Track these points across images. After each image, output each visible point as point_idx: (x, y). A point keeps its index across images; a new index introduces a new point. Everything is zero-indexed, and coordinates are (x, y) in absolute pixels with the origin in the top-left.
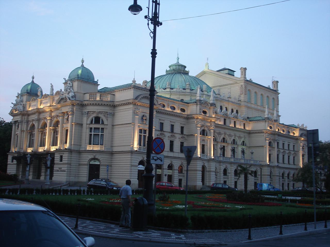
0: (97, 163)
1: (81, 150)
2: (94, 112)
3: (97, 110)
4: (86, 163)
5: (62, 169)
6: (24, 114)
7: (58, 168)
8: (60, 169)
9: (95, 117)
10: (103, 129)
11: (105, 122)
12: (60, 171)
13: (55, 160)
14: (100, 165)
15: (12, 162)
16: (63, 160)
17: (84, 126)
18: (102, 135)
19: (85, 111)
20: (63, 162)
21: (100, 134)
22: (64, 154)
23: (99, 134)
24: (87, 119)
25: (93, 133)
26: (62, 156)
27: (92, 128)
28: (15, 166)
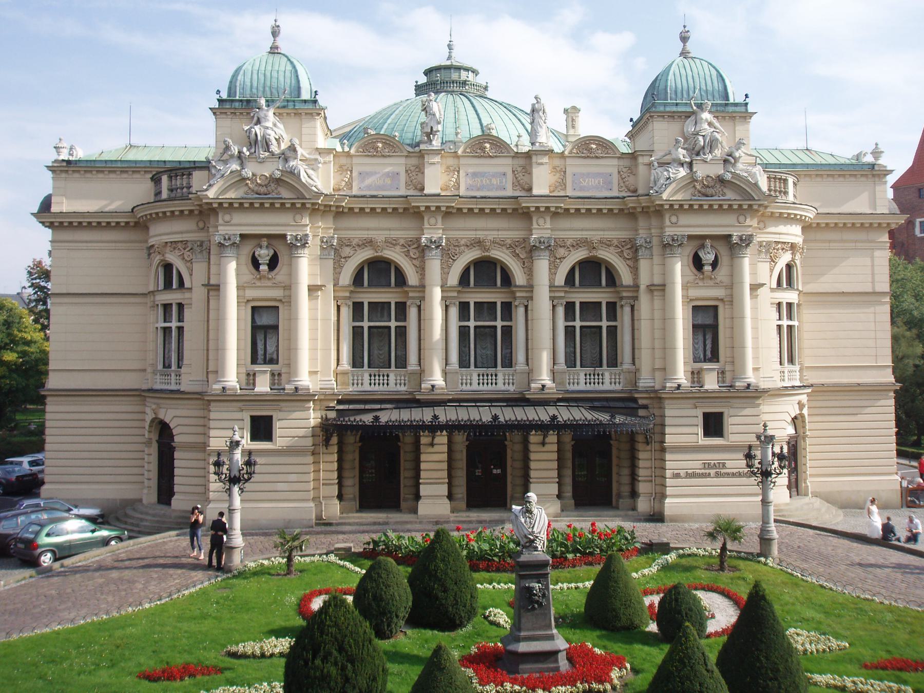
6: (325, 206)
7: (698, 464)
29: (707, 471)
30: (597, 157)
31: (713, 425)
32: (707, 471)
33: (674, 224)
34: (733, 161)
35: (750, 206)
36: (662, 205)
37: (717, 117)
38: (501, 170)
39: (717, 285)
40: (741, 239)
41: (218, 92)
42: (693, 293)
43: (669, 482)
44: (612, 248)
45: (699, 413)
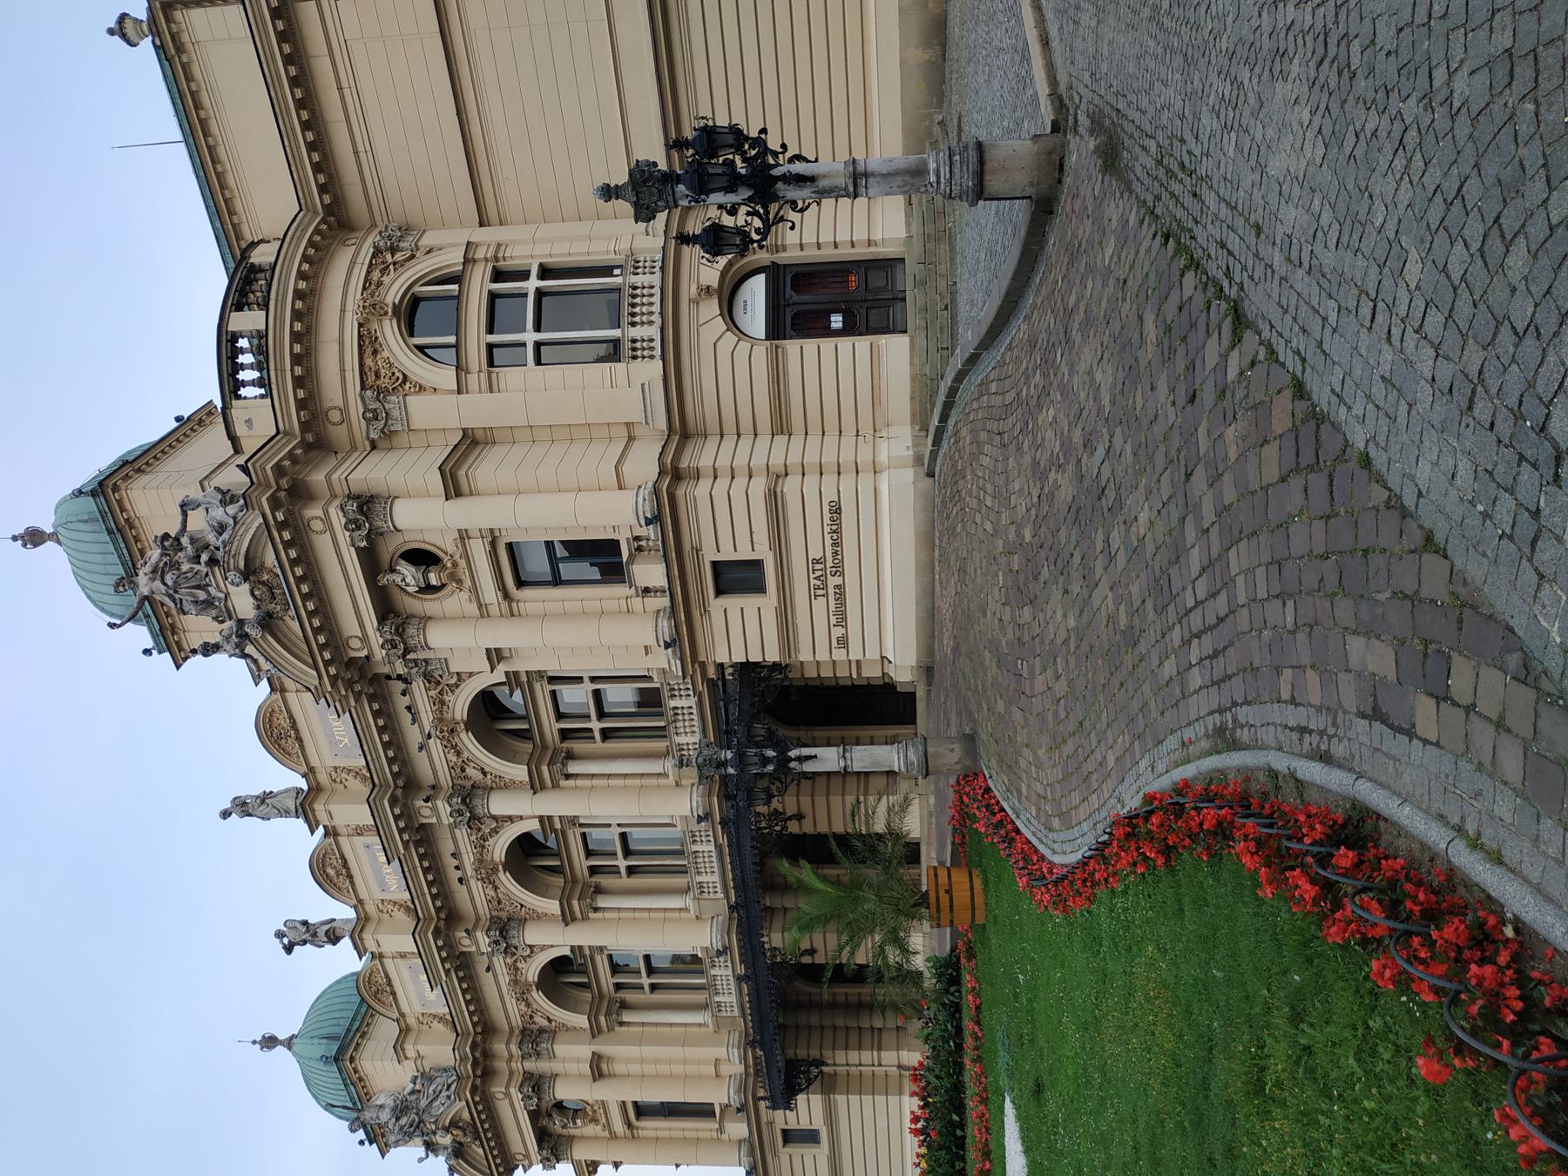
0: (756, 288)
1: (662, 424)
2: (368, 343)
3: (349, 315)
4: (761, 351)
5: (815, 553)
6: (475, 1064)
8: (818, 588)
9: (412, 335)
10: (499, 275)
11: (452, 259)
12: (838, 580)
13: (755, 657)
14: (775, 273)
15: (811, 1137)
16: (744, 554)
17: (478, 409)
18: (545, 272)
19: (361, 410)
20: (764, 552)
21: (533, 283)
22: (697, 550)
23: (540, 294)
24: (422, 389)
25: (530, 337)
26: (715, 564)
27: (491, 347)
28: (840, 1099)
29: (831, 591)
30: (294, 725)
31: (737, 577)
32: (831, 591)
33: (364, 638)
34: (204, 557)
35: (281, 526)
36: (334, 680)
37: (142, 553)
38: (361, 850)
39: (466, 555)
40: (359, 528)
41: (361, 1143)
42: (490, 593)
43: (855, 654)
44: (446, 698)
45: (717, 605)
